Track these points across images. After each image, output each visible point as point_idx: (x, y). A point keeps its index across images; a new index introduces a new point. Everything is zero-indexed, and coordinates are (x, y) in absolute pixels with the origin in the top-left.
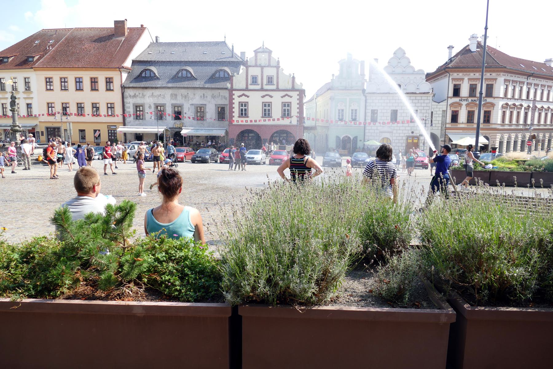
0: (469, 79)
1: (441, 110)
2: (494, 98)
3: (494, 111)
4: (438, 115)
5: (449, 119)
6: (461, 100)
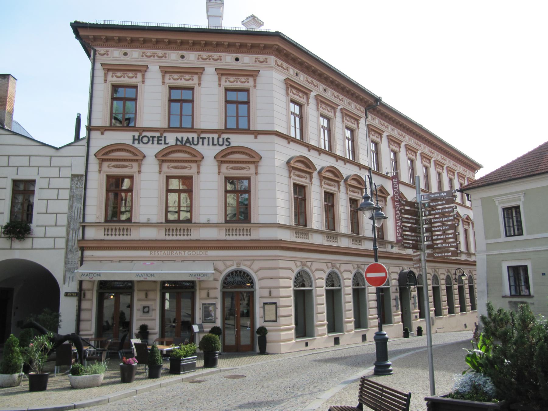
0: (166, 71)
1: (66, 173)
2: (257, 133)
3: (261, 177)
4: (53, 194)
5: (95, 209)
6: (140, 140)
